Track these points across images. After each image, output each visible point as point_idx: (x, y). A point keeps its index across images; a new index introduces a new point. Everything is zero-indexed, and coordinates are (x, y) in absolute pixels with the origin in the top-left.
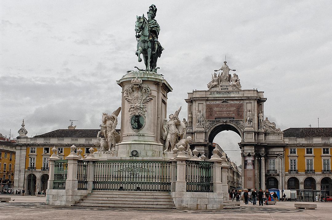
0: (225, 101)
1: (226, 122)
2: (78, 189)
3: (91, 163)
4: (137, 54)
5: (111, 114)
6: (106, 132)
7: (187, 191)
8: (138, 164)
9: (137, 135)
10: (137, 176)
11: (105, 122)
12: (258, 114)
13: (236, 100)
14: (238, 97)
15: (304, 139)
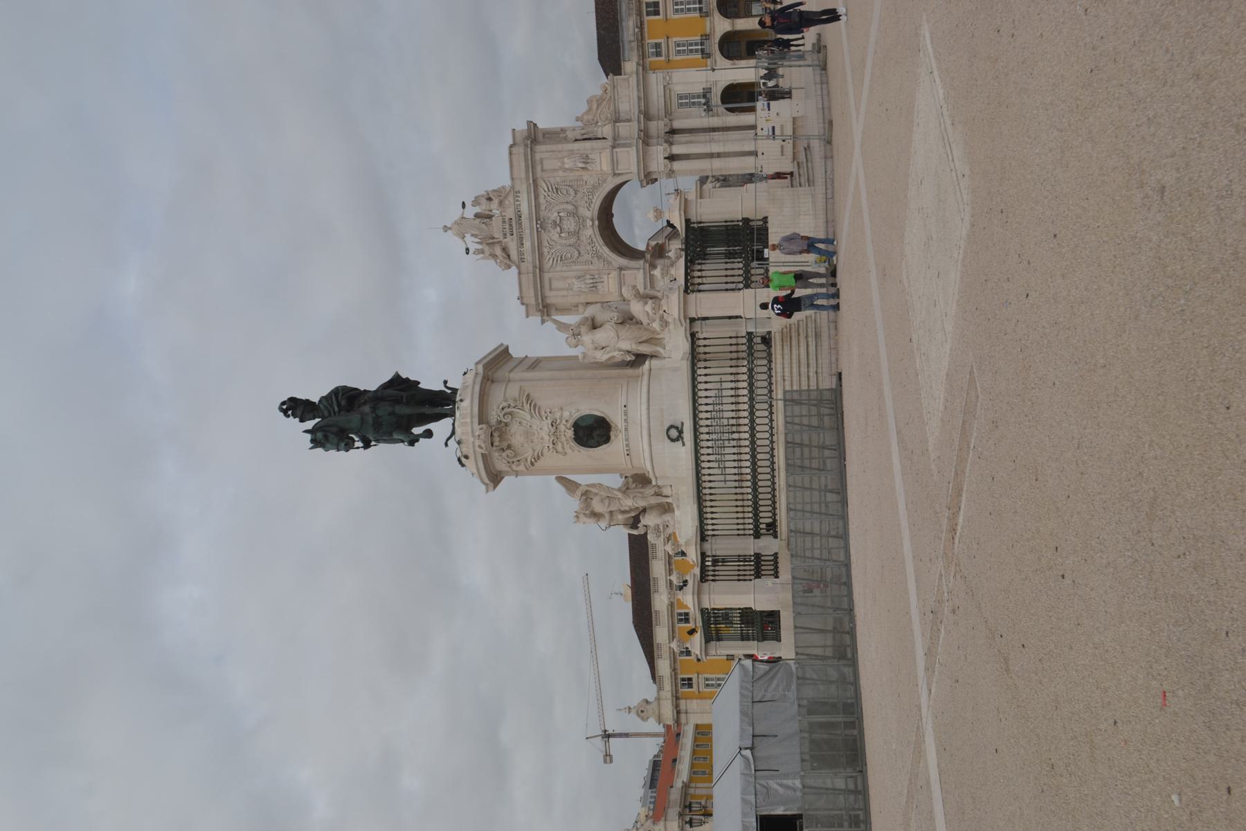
0: (541, 224)
1: (592, 220)
2: (777, 577)
3: (707, 546)
4: (412, 443)
5: (574, 503)
6: (624, 512)
8: (702, 423)
9: (626, 429)
10: (734, 422)
11: (596, 516)
12: (566, 140)
13: (536, 197)
14: (529, 193)
15: (624, 24)
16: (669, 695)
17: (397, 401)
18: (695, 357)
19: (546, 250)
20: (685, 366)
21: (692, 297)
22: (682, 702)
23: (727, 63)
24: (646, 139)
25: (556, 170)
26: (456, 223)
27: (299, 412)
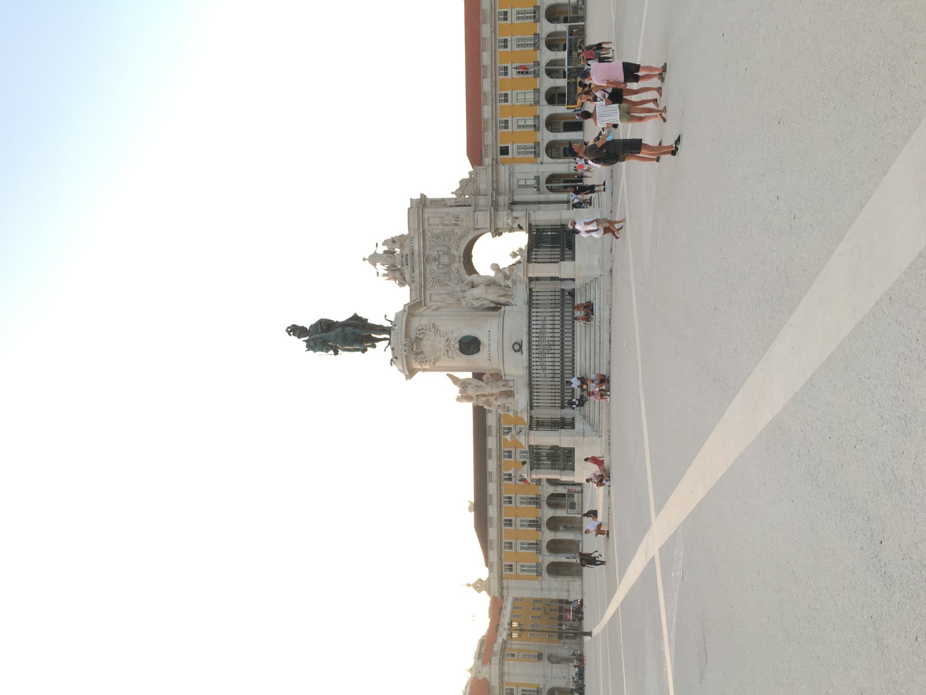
3: (533, 412)
5: (456, 390)
7: (574, 260)
12: (445, 205)
13: (424, 241)
15: (486, 134)
16: (496, 576)
17: (356, 327)
18: (530, 304)
19: (428, 276)
20: (525, 308)
21: (531, 265)
22: (505, 582)
23: (551, 160)
24: (495, 205)
25: (437, 225)
26: (370, 257)
27: (297, 333)
